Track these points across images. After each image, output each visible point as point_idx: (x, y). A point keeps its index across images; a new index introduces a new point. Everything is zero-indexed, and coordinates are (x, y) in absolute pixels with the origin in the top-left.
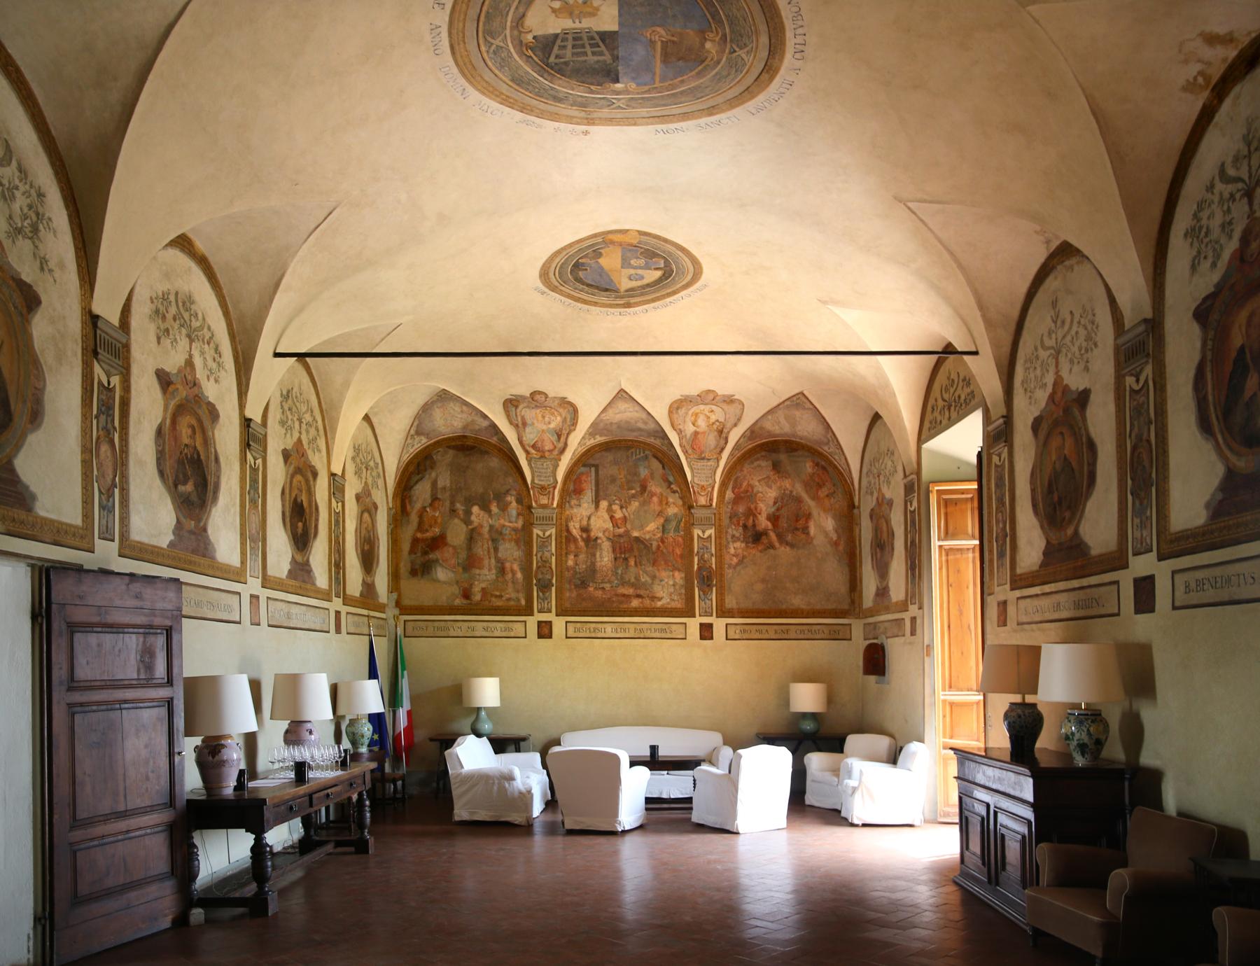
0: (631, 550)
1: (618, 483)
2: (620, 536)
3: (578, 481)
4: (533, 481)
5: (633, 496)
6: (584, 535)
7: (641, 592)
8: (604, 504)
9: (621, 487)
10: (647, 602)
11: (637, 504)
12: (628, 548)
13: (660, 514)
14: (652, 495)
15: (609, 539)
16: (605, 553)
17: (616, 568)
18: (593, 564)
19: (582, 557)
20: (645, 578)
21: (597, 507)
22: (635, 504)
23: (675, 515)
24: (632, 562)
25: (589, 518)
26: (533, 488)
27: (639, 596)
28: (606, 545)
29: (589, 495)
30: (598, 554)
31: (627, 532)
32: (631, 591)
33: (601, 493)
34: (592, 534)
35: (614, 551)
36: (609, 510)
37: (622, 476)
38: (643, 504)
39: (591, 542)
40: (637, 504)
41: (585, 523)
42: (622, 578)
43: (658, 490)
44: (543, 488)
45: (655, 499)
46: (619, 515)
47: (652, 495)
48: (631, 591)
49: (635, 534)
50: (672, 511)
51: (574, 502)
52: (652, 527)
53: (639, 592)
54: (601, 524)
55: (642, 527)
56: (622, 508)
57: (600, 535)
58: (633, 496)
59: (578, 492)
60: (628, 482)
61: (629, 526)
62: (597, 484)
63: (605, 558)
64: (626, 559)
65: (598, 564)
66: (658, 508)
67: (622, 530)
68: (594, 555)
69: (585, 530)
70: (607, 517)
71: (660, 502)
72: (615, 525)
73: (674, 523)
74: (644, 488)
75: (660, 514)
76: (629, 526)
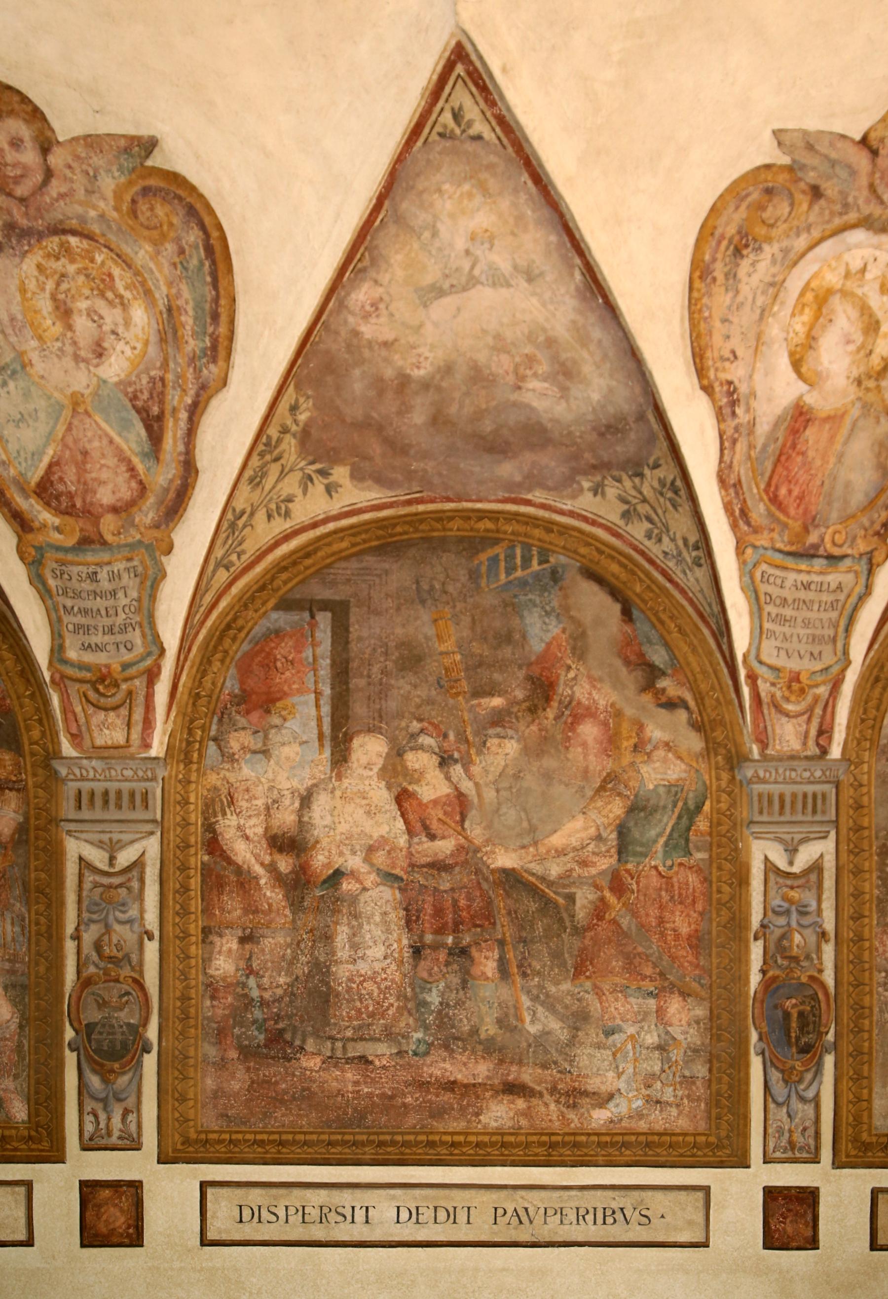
0: (487, 916)
1: (432, 667)
2: (439, 866)
3: (261, 659)
4: (57, 651)
5: (498, 719)
6: (285, 864)
7: (527, 1075)
8: (369, 750)
9: (446, 684)
10: (550, 1113)
11: (512, 747)
12: (463, 912)
13: (609, 784)
14: (576, 714)
15: (389, 878)
16: (372, 931)
17: (425, 985)
18: (321, 970)
19: (275, 943)
20: (538, 1022)
21: (341, 757)
22: (505, 751)
23: (674, 789)
24: (487, 964)
25: (306, 800)
26: (60, 681)
27: (513, 1089)
28: (379, 902)
29: (303, 717)
30: (342, 934)
31: (467, 854)
32: (481, 1070)
33: (359, 709)
34: (319, 860)
35: (411, 920)
36: (394, 770)
37: (445, 639)
38: (535, 750)
39: (313, 888)
40: (512, 747)
41: (286, 818)
42: (443, 1019)
43: (603, 697)
44: (102, 680)
45: (589, 731)
46: (433, 787)
47: (576, 714)
48: (481, 1070)
49: (504, 860)
50: (658, 774)
51: (235, 741)
52: (573, 831)
53: (513, 1074)
54: (355, 820)
55: (531, 835)
56: (445, 761)
57: (354, 862)
58: (498, 719)
59: (260, 700)
60: (475, 665)
61: (476, 831)
62: (341, 672)
63: (372, 947)
64: (462, 952)
65: (342, 972)
66: (599, 765)
67: (445, 847)
68: (328, 938)
69: (289, 843)
70: (382, 795)
71: (611, 742)
72: (418, 824)
73: (667, 821)
74: (542, 688)
75: (609, 784)
76: (476, 831)
